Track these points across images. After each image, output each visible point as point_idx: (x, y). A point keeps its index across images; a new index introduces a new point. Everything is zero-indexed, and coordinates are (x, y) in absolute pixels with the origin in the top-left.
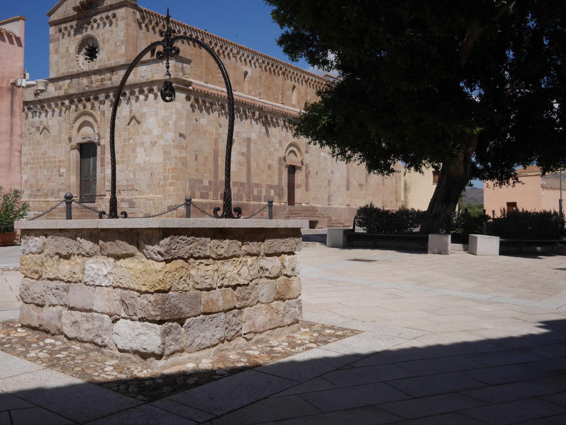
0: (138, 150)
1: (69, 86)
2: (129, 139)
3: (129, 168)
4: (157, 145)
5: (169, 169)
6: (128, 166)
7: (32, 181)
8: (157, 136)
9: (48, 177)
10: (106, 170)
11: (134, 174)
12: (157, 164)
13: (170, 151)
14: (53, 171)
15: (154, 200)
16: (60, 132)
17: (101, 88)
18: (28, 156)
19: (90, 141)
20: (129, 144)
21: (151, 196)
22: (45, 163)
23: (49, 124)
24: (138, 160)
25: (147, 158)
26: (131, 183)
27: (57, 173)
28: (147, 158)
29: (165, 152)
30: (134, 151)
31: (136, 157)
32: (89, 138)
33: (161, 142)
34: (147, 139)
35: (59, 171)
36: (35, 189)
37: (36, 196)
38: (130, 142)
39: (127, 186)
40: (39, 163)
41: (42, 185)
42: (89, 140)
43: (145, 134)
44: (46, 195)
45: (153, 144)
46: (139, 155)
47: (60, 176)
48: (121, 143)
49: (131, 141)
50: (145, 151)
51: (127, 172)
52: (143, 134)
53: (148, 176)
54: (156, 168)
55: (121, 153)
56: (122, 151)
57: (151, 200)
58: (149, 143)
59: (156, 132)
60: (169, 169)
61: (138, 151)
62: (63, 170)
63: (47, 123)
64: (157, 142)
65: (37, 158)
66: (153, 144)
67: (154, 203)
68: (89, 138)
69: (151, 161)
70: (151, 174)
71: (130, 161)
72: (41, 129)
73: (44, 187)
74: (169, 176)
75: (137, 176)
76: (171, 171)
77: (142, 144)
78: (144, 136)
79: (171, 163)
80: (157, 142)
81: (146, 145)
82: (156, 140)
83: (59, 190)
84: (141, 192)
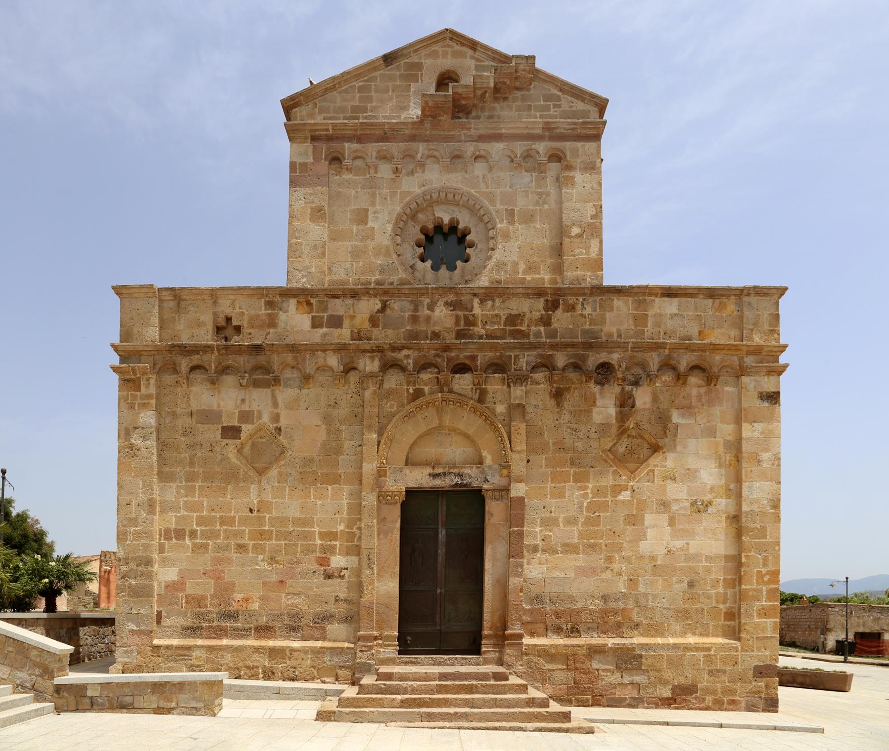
0: (649, 519)
1: (373, 321)
2: (617, 490)
3: (616, 566)
4: (710, 510)
5: (760, 575)
6: (609, 559)
7: (204, 587)
9: (274, 578)
10: (525, 566)
11: (632, 582)
12: (709, 559)
13: (764, 529)
14: (298, 562)
15: (709, 649)
18: (183, 513)
19: (461, 485)
20: (616, 503)
21: (691, 640)
24: (645, 547)
25: (678, 544)
27: (315, 567)
28: (678, 544)
30: (634, 520)
31: (643, 536)
32: (461, 476)
34: (677, 492)
35: (323, 562)
36: (212, 609)
37: (220, 632)
38: (621, 497)
39: (604, 613)
42: (457, 480)
43: (674, 479)
44: (264, 631)
45: (700, 507)
46: (650, 533)
47: (329, 576)
48: (585, 496)
49: (625, 496)
51: (608, 575)
52: (665, 479)
53: (678, 587)
54: (708, 570)
55: (584, 524)
56: (587, 518)
57: (697, 649)
58: (687, 504)
60: (760, 575)
61: (646, 523)
62: (338, 561)
63: (276, 418)
64: (710, 503)
67: (709, 659)
68: (461, 476)
69: (692, 551)
70: (691, 585)
71: (620, 549)
73: (255, 606)
74: (761, 591)
75: (642, 589)
76: (766, 579)
77: (664, 505)
78: (670, 486)
79: (765, 560)
80: (710, 503)
81: (674, 507)
82: (709, 497)
83: (328, 617)
84: (655, 629)
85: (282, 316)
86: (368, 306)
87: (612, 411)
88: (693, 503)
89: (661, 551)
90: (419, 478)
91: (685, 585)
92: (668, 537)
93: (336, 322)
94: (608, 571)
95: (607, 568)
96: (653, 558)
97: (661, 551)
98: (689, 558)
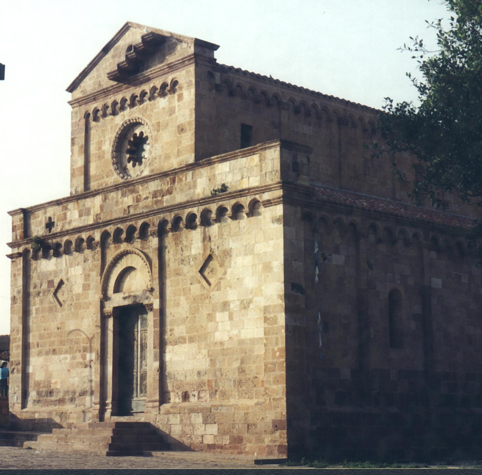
0: (219, 316)
1: (102, 207)
4: (251, 306)
8: (252, 290)
16: (86, 287)
17: (156, 207)
22: (62, 343)
23: (69, 274)
25: (235, 332)
26: (205, 378)
27: (81, 360)
29: (266, 319)
30: (211, 317)
33: (260, 302)
34: (232, 296)
35: (84, 358)
40: (53, 343)
41: (56, 383)
44: (61, 401)
45: (245, 305)
50: (231, 318)
58: (238, 303)
59: (250, 282)
63: (67, 273)
64: (250, 302)
65: (50, 335)
66: (245, 305)
69: (243, 337)
72: (56, 285)
73: (58, 386)
76: (278, 354)
81: (232, 306)
82: (250, 297)
85: (69, 214)
86: (98, 200)
87: (200, 245)
88: (242, 302)
89: (226, 338)
90: (117, 300)
91: (239, 361)
92: (228, 328)
93: (88, 212)
94: (200, 354)
95: (200, 352)
96: (222, 343)
97: (226, 338)
98: (241, 342)
